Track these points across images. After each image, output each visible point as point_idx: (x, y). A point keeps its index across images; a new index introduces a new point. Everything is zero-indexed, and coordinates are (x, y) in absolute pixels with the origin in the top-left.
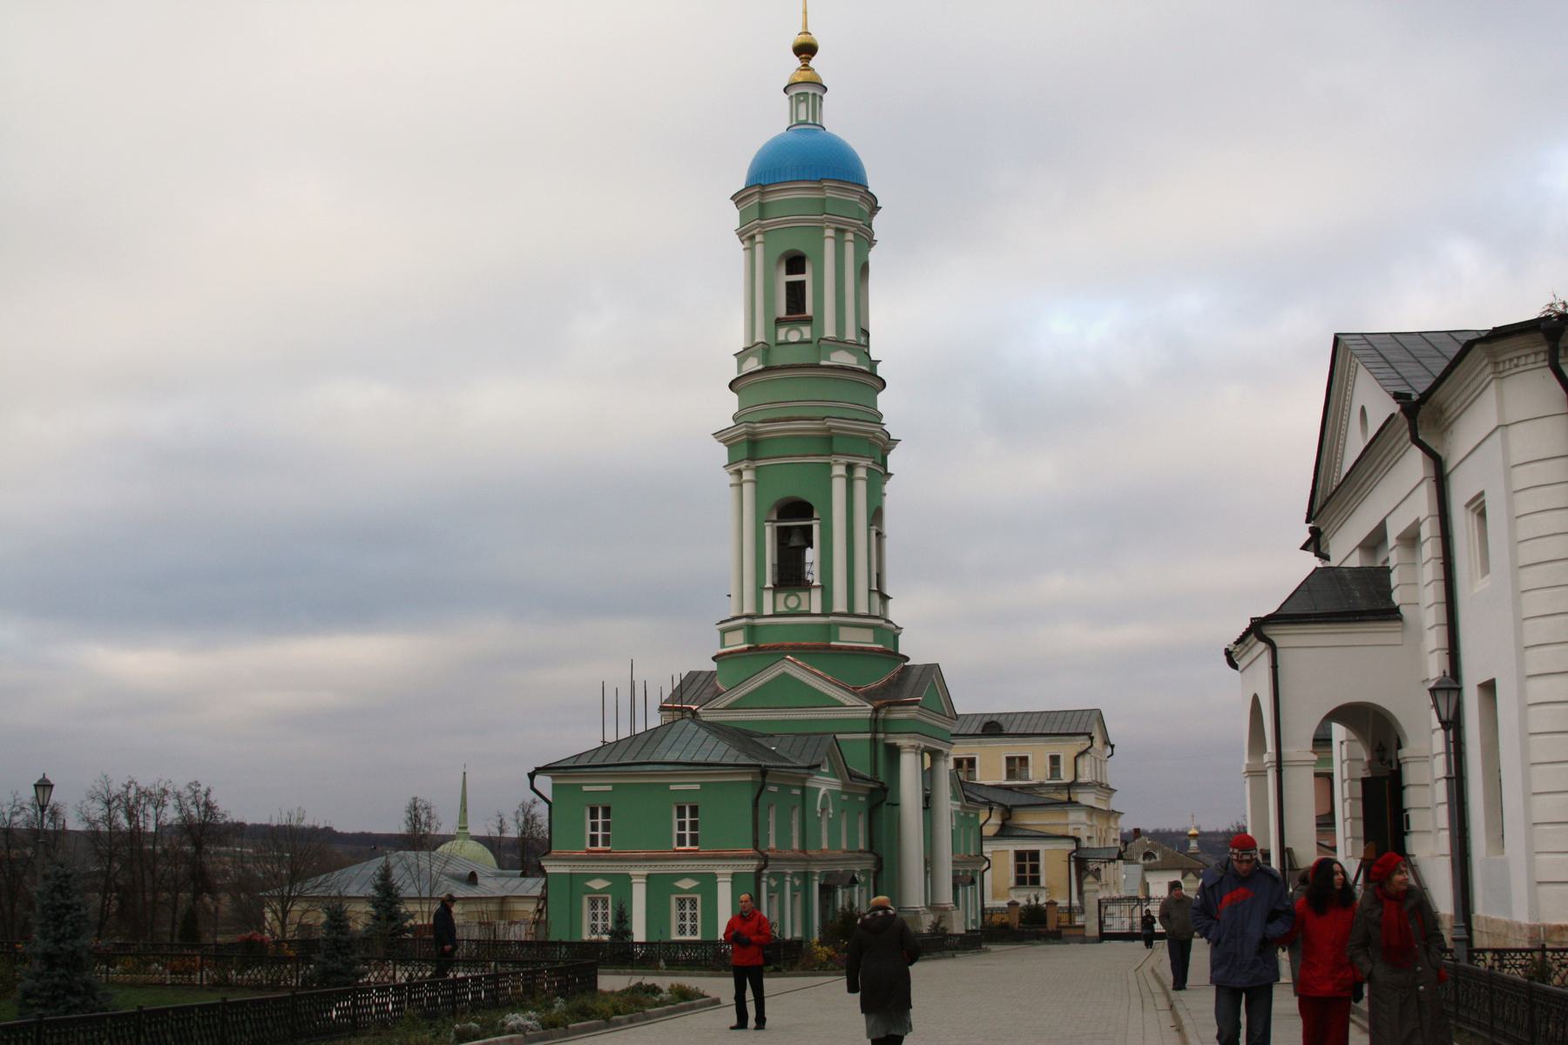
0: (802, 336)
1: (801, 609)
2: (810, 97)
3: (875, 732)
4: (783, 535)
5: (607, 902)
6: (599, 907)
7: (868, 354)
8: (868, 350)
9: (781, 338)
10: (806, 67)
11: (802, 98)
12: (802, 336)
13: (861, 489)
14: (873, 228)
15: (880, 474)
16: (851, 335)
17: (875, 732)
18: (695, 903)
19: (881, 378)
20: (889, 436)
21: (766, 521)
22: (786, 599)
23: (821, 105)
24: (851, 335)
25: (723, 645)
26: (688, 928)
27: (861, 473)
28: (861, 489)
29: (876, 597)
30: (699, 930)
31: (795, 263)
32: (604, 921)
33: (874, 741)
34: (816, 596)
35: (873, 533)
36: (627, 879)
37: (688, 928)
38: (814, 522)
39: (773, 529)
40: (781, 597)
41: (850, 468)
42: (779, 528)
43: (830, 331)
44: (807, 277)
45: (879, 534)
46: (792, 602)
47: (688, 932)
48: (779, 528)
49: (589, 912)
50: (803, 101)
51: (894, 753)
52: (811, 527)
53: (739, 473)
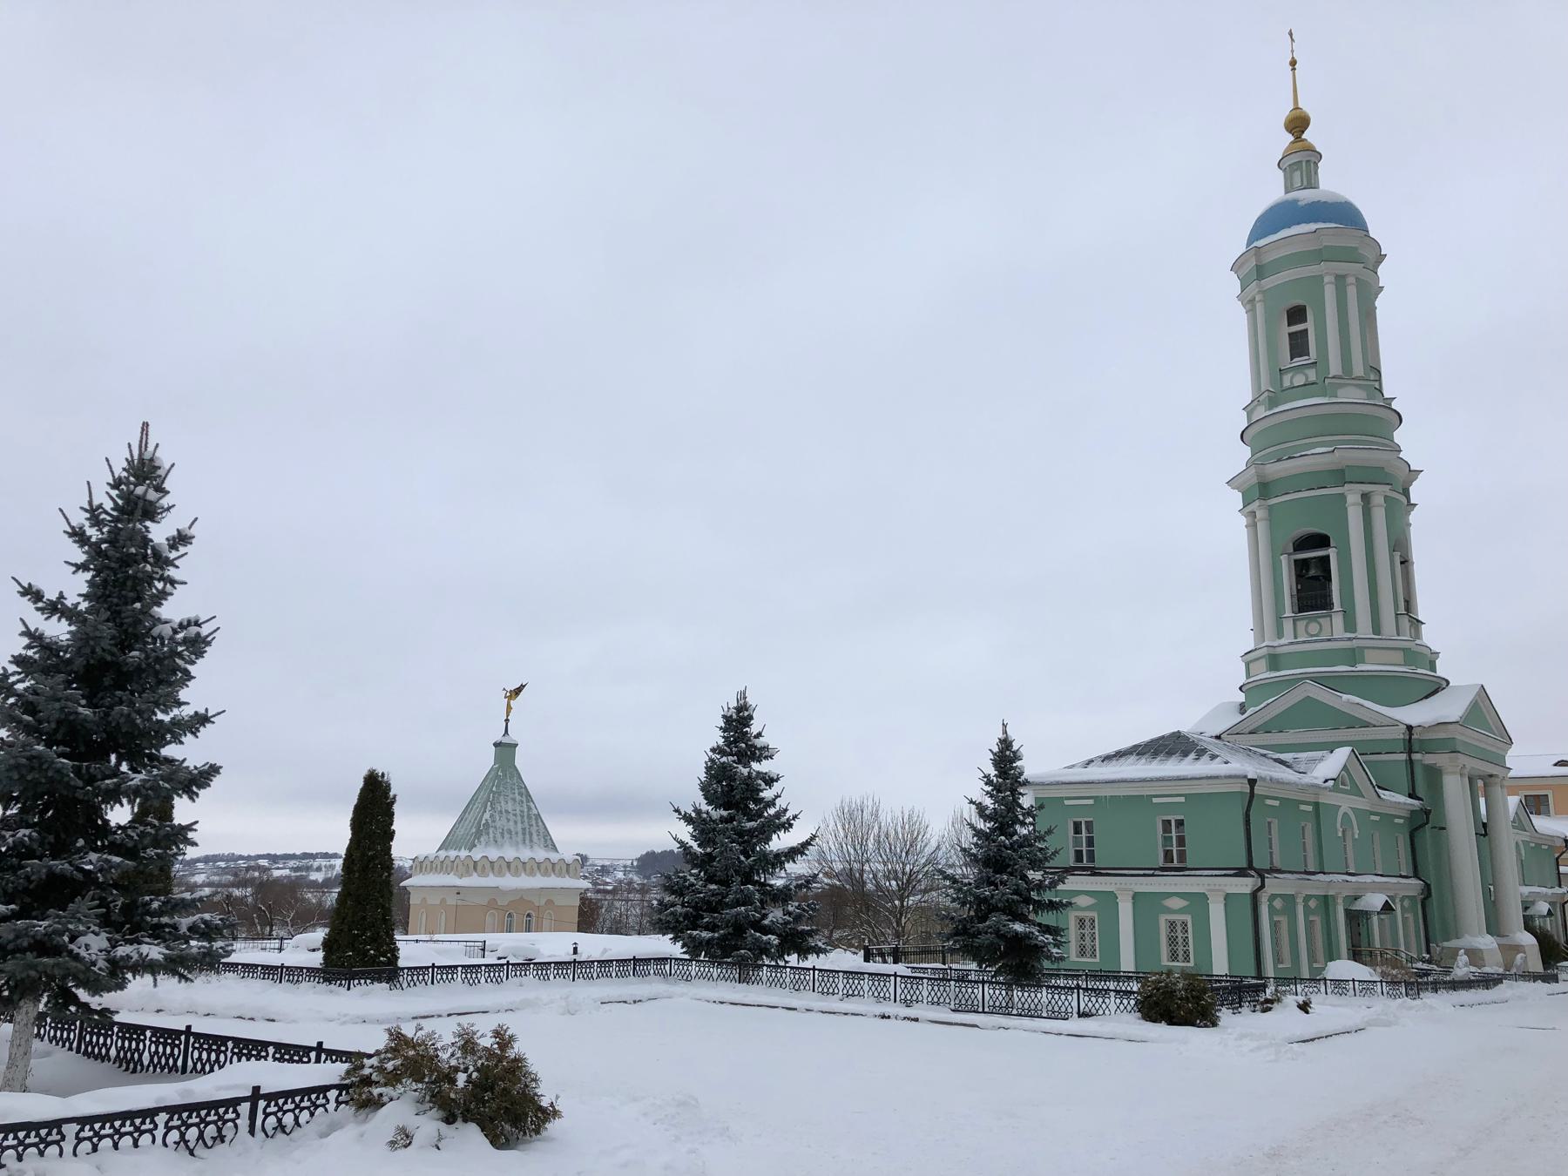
0: (1307, 378)
1: (1305, 622)
2: (1304, 164)
3: (1410, 752)
4: (1301, 567)
5: (1094, 921)
6: (1179, 931)
7: (1380, 391)
8: (1380, 385)
9: (1287, 383)
10: (1298, 138)
11: (1295, 167)
12: (1307, 378)
13: (1379, 515)
14: (1378, 274)
15: (1400, 505)
16: (1359, 370)
17: (1410, 752)
18: (1186, 925)
19: (1395, 411)
20: (1409, 466)
21: (1282, 555)
22: (1307, 626)
23: (1316, 173)
24: (1359, 370)
25: (1248, 676)
26: (1181, 953)
27: (1378, 500)
28: (1379, 515)
29: (1405, 621)
30: (1191, 956)
31: (1296, 314)
32: (1185, 946)
33: (1411, 762)
34: (1338, 621)
35: (1398, 560)
36: (1111, 897)
37: (1181, 953)
38: (1330, 550)
39: (1289, 561)
40: (1301, 625)
41: (1366, 497)
42: (1295, 561)
43: (1335, 368)
44: (1309, 325)
45: (1405, 562)
46: (1314, 628)
47: (1181, 957)
48: (1295, 561)
49: (1076, 932)
50: (1297, 170)
51: (1434, 774)
52: (1328, 557)
53: (1253, 514)
